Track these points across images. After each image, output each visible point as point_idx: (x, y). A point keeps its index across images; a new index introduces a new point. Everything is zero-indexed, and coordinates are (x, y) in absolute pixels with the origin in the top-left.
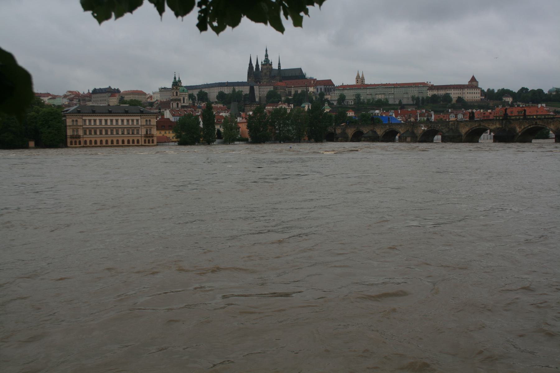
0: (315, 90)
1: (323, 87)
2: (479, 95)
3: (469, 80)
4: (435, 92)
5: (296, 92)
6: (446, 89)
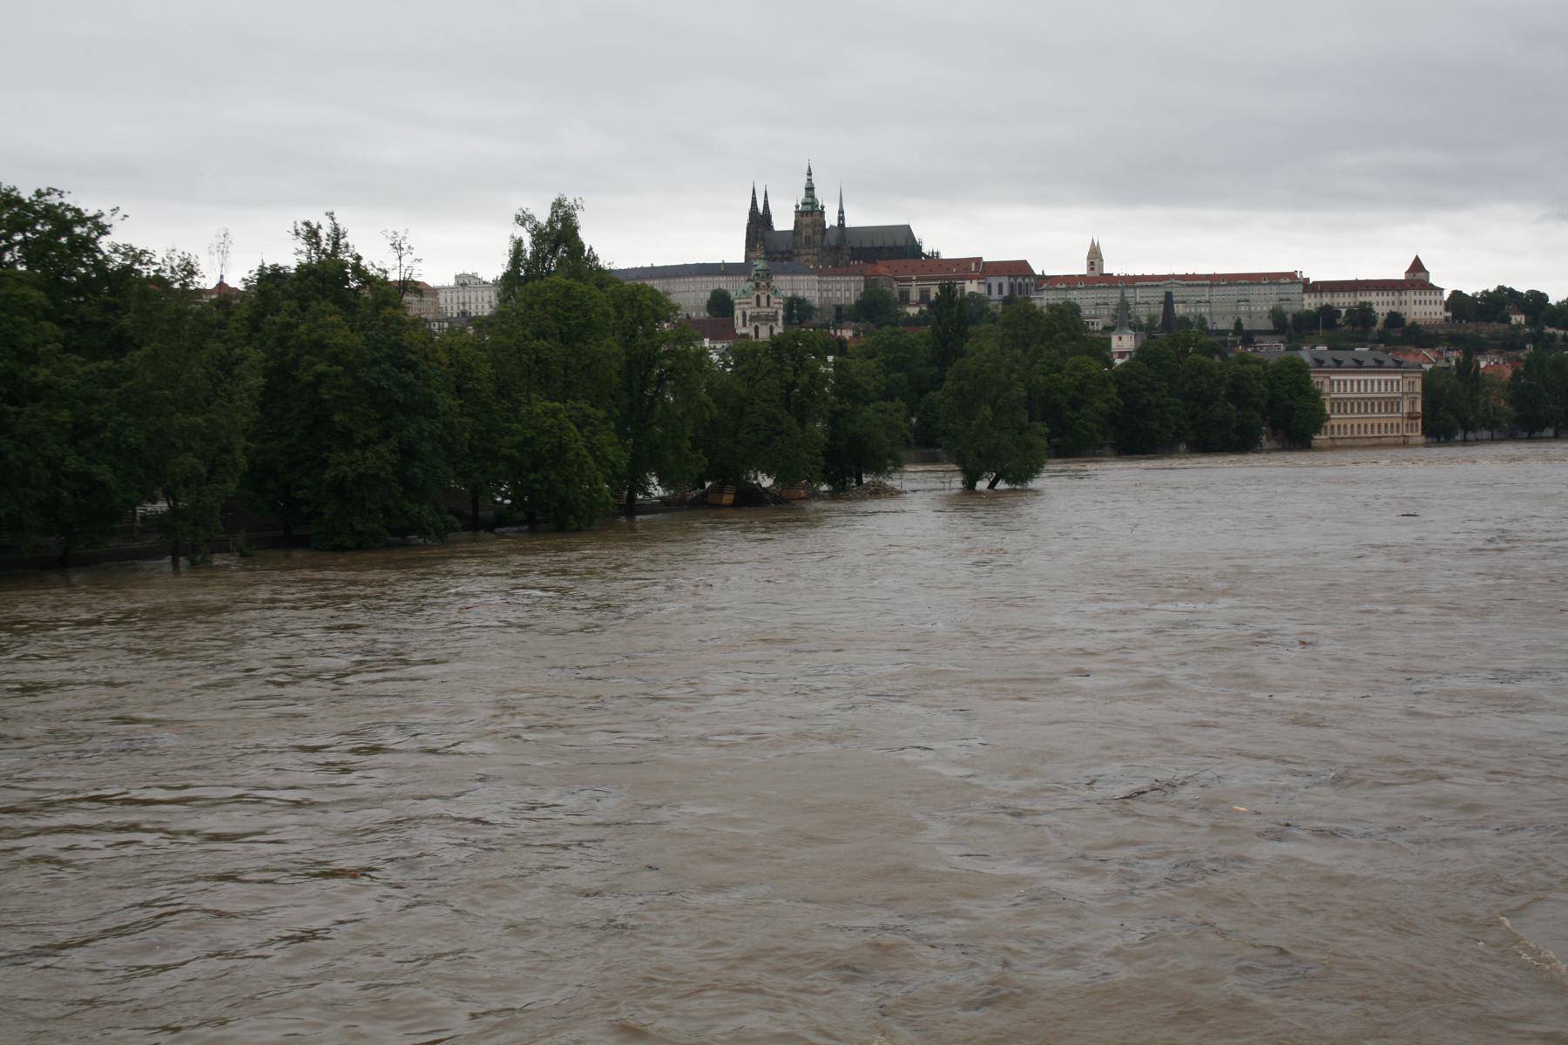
1: (1005, 281)
2: (1442, 308)
4: (1326, 299)
5: (924, 296)
6: (1321, 291)
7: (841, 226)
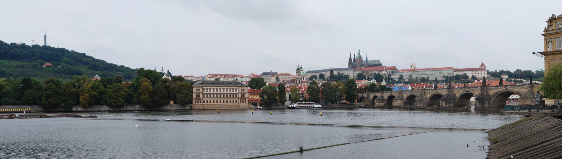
1: (390, 71)
4: (458, 73)
7: (367, 61)
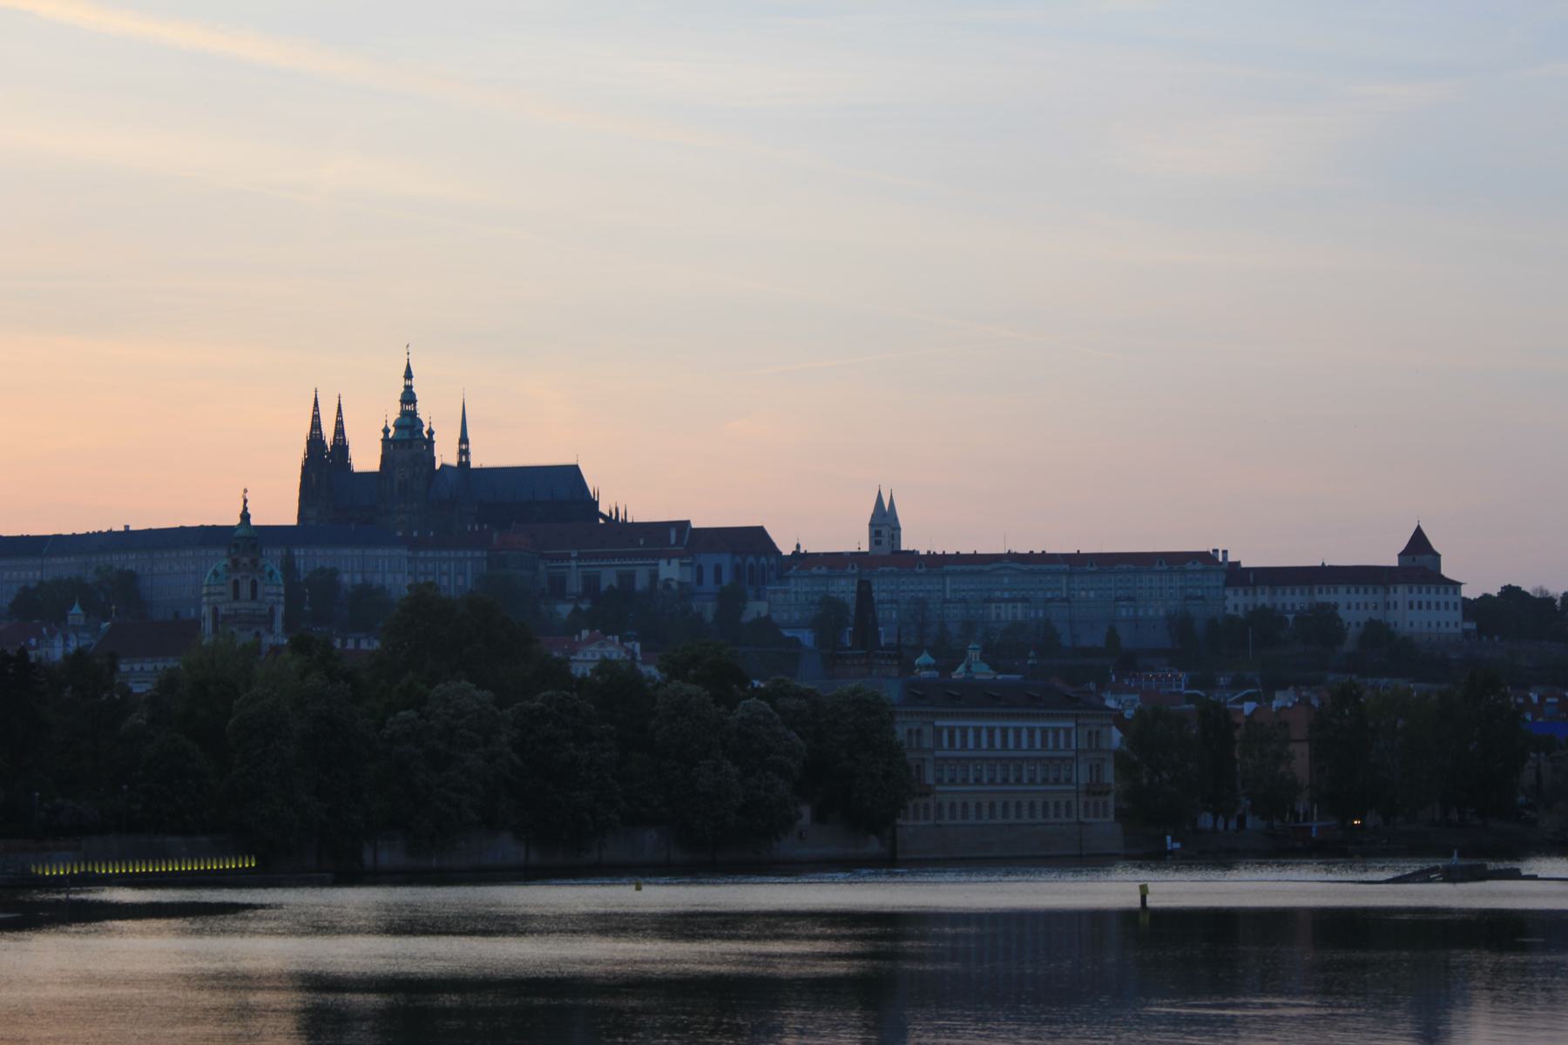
0: (688, 576)
1: (726, 560)
2: (1457, 615)
3: (1402, 548)
4: (1263, 598)
5: (591, 584)
7: (464, 465)
